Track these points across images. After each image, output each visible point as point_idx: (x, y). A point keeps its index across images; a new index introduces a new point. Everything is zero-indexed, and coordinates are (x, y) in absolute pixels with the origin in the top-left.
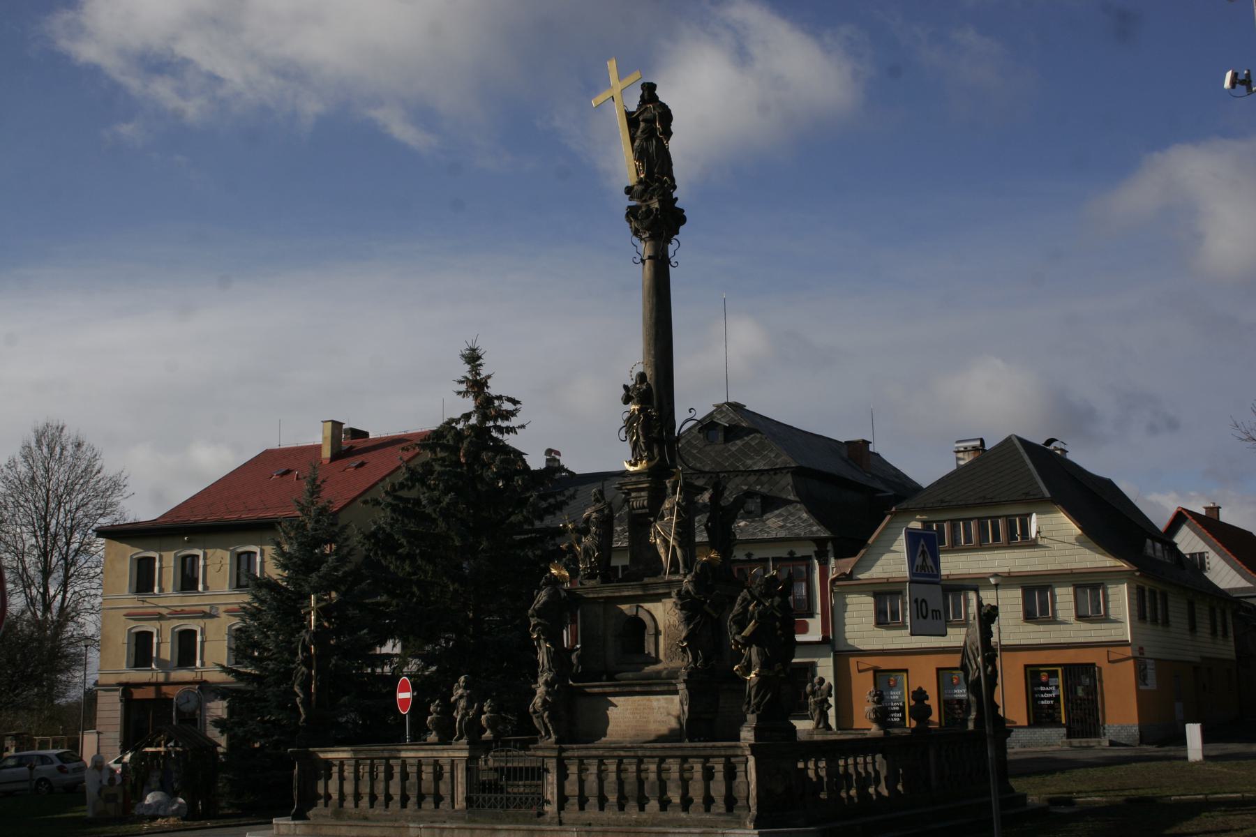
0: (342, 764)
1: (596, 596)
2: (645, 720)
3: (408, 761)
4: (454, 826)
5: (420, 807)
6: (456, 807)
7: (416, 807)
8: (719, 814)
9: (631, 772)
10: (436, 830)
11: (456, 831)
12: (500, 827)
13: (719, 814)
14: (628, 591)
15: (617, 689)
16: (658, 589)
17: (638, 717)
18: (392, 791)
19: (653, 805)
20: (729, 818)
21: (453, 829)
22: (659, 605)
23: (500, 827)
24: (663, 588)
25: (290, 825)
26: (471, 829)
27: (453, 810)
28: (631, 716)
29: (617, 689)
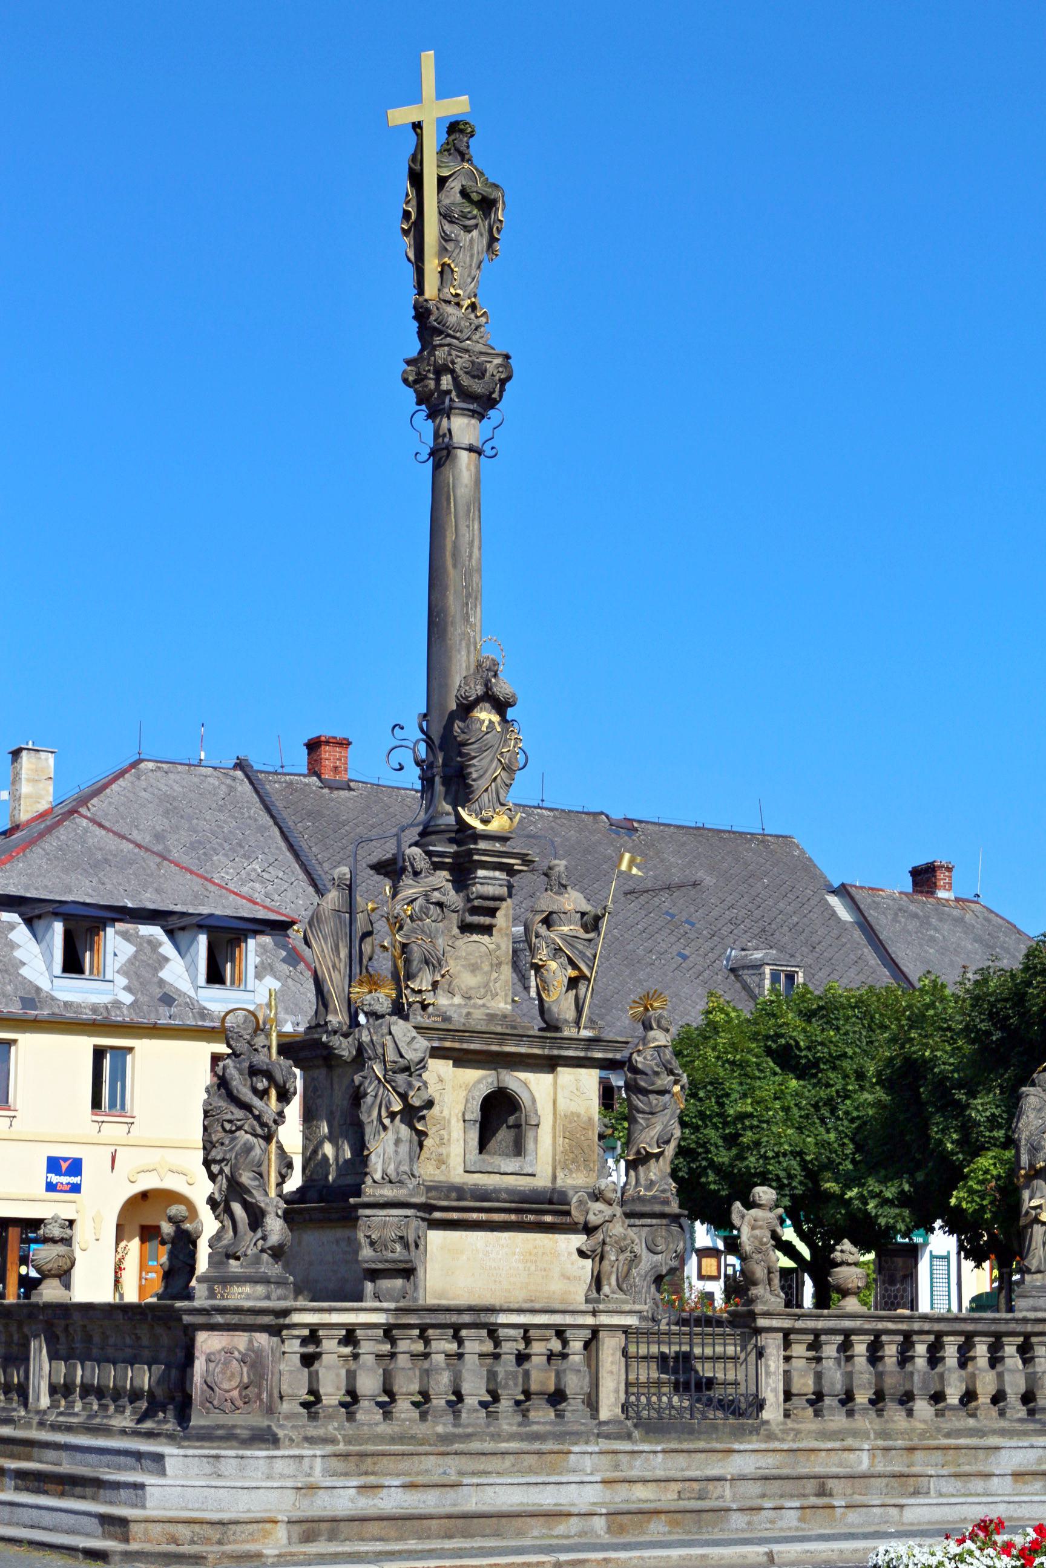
0: (350, 1337)
1: (457, 1045)
2: (544, 1273)
3: (502, 1332)
4: (659, 1448)
5: (525, 1414)
6: (604, 1414)
7: (519, 1419)
8: (1021, 1420)
9: (891, 1356)
10: (620, 1456)
11: (660, 1455)
12: (737, 1446)
13: (1021, 1420)
14: (517, 1045)
15: (513, 1217)
16: (567, 1049)
17: (533, 1268)
18: (466, 1389)
19: (922, 1407)
20: (1031, 1426)
21: (655, 1452)
22: (546, 1079)
23: (742, 1447)
24: (576, 1049)
25: (302, 1457)
26: (689, 1452)
27: (595, 1422)
28: (521, 1266)
29: (513, 1217)
